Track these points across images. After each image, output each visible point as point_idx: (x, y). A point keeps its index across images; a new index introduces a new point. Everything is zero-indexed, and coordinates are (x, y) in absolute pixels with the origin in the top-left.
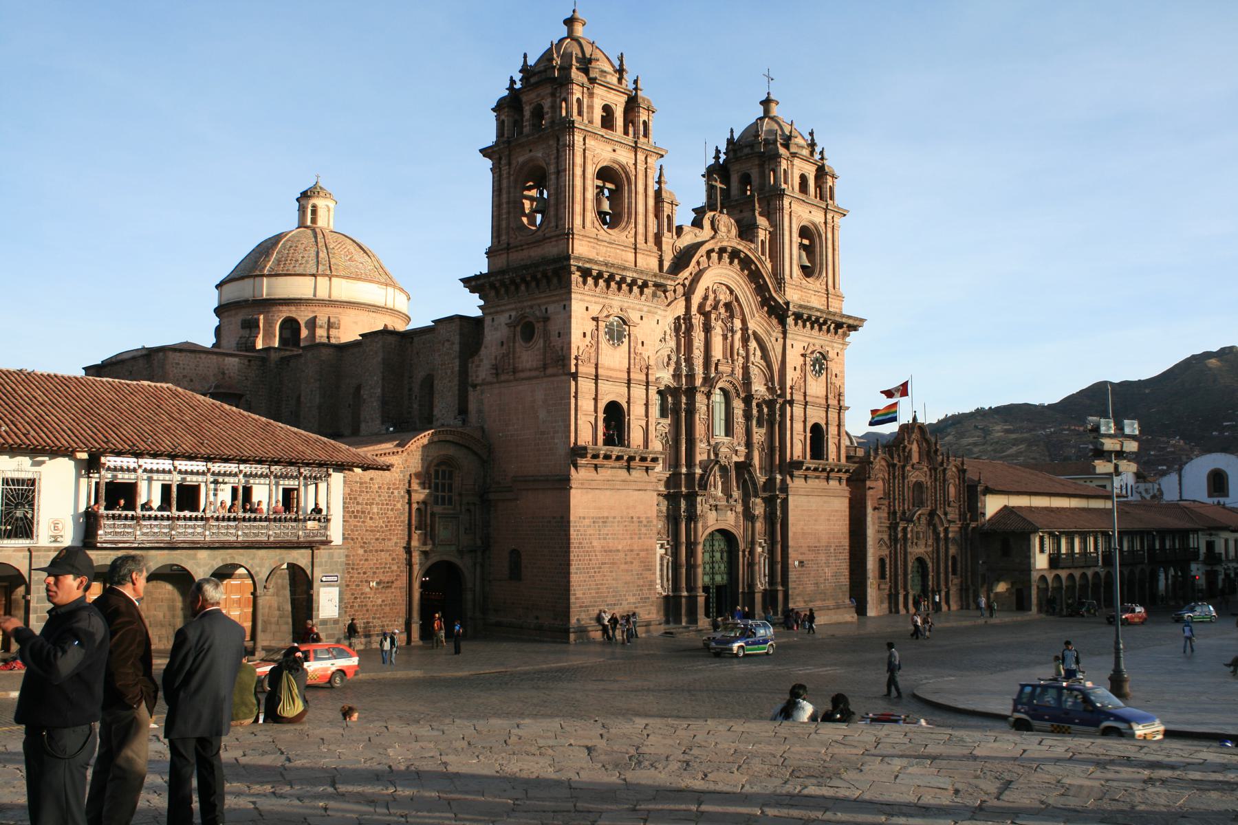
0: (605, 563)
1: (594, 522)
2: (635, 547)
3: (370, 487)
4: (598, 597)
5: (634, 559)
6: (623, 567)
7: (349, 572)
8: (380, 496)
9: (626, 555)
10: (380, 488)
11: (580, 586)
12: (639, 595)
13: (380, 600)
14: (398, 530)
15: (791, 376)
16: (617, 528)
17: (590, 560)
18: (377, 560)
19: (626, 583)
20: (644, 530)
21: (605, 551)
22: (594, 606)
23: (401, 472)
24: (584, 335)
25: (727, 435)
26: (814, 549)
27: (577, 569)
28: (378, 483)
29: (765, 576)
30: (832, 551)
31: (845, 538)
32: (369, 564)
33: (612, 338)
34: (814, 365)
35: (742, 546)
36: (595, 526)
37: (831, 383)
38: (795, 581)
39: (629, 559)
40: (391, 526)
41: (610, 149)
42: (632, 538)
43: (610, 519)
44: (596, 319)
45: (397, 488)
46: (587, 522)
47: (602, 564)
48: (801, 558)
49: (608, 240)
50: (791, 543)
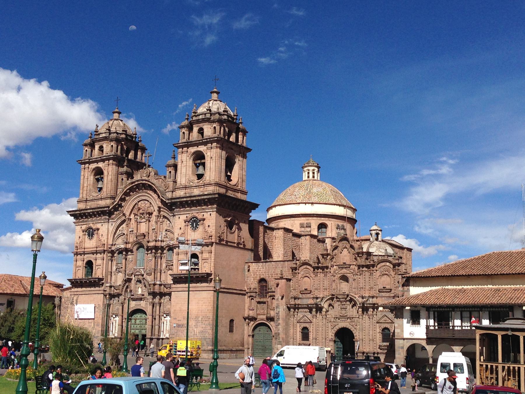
15: (177, 232)
30: (200, 319)
31: (210, 313)
33: (89, 236)
34: (192, 225)
38: (174, 334)
48: (178, 322)
49: (92, 199)
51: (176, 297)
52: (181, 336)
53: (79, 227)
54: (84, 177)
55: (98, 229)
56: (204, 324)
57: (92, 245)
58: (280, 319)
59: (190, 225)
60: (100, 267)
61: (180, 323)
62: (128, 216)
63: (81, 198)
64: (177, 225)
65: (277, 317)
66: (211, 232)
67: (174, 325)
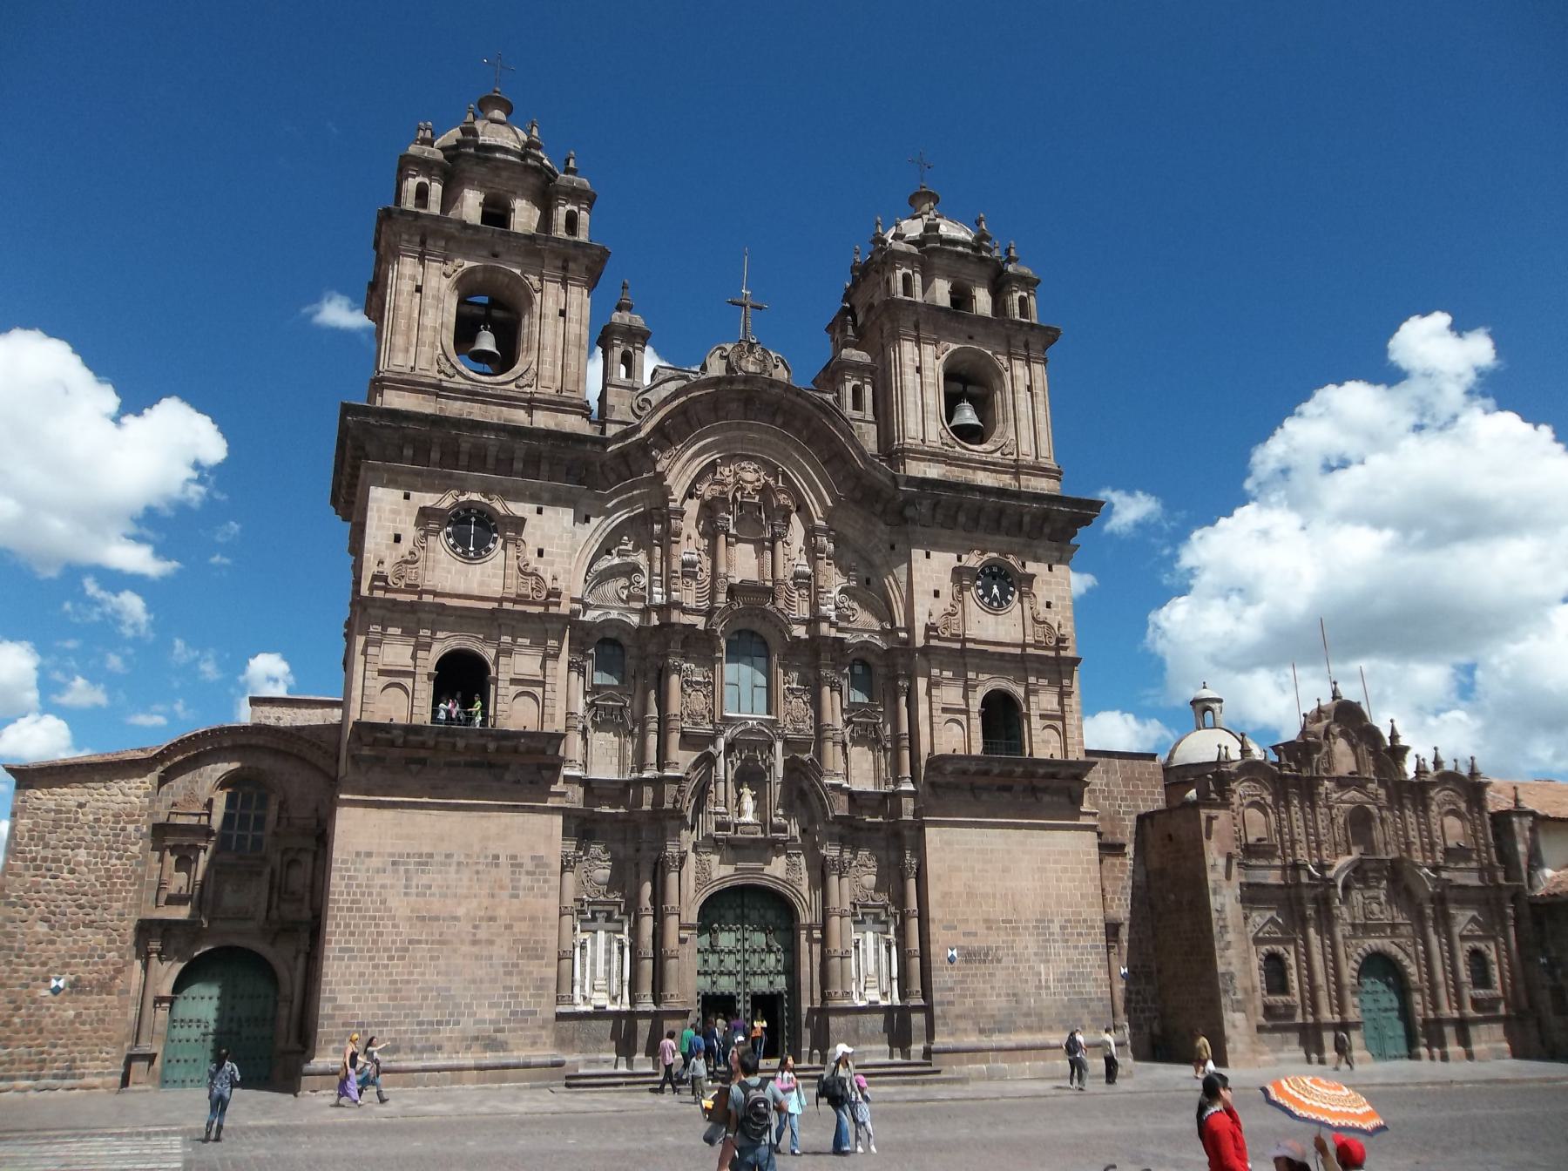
0: (419, 942)
1: (394, 863)
2: (501, 912)
3: (76, 820)
4: (395, 1007)
5: (499, 935)
6: (466, 948)
7: (9, 963)
8: (95, 834)
9: (475, 927)
10: (97, 820)
11: (347, 983)
12: (508, 1005)
13: (72, 1013)
14: (130, 891)
16: (452, 875)
17: (380, 934)
18: (75, 942)
19: (474, 981)
20: (525, 880)
21: (423, 919)
22: (386, 1024)
23: (146, 796)
24: (397, 539)
25: (769, 713)
26: (1012, 926)
27: (341, 950)
28: (94, 814)
29: (891, 979)
30: (1055, 928)
31: (1091, 905)
32: (57, 951)
33: (461, 540)
35: (806, 918)
36: (396, 871)
37: (1033, 618)
38: (951, 989)
39: (482, 934)
40: (114, 884)
41: (485, 253)
42: (493, 896)
43: (436, 858)
44: (425, 515)
45: (136, 821)
46: (375, 862)
47: (410, 942)
48: (963, 941)
49: (469, 387)
50: (934, 912)
51: (949, 843)
52: (984, 995)
53: (401, 493)
54: (419, 289)
55: (519, 524)
56: (1076, 947)
57: (482, 584)
58: (1230, 929)
59: (978, 588)
60: (538, 691)
61: (975, 944)
62: (678, 504)
63: (407, 370)
64: (921, 576)
65: (1221, 923)
66: (1059, 627)
67: (950, 953)
